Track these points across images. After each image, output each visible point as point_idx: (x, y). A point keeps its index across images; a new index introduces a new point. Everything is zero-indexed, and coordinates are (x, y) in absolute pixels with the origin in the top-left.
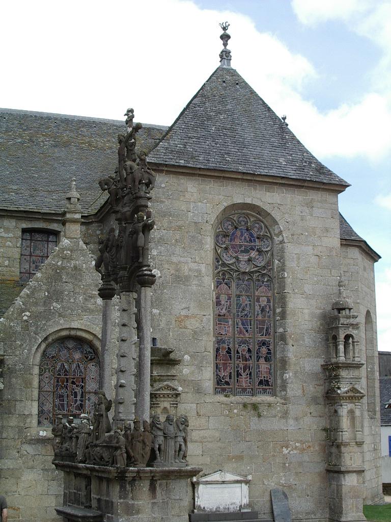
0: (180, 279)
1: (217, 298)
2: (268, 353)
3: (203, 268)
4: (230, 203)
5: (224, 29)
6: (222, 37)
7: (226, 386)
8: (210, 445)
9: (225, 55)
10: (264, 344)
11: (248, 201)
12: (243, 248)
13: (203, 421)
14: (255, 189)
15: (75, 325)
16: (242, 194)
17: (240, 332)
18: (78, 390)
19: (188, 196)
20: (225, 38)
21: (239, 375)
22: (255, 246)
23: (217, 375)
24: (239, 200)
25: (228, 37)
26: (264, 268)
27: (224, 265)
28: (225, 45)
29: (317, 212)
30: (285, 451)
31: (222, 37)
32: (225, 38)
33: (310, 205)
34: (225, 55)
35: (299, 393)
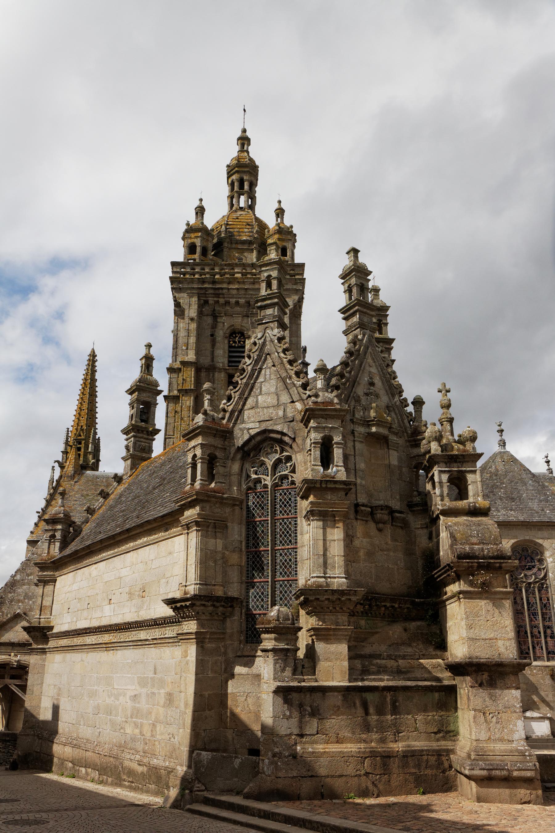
2: (552, 633)
7: (527, 655)
10: (548, 628)
11: (527, 538)
12: (527, 567)
14: (531, 530)
22: (535, 565)
23: (520, 648)
25: (502, 431)
26: (542, 579)
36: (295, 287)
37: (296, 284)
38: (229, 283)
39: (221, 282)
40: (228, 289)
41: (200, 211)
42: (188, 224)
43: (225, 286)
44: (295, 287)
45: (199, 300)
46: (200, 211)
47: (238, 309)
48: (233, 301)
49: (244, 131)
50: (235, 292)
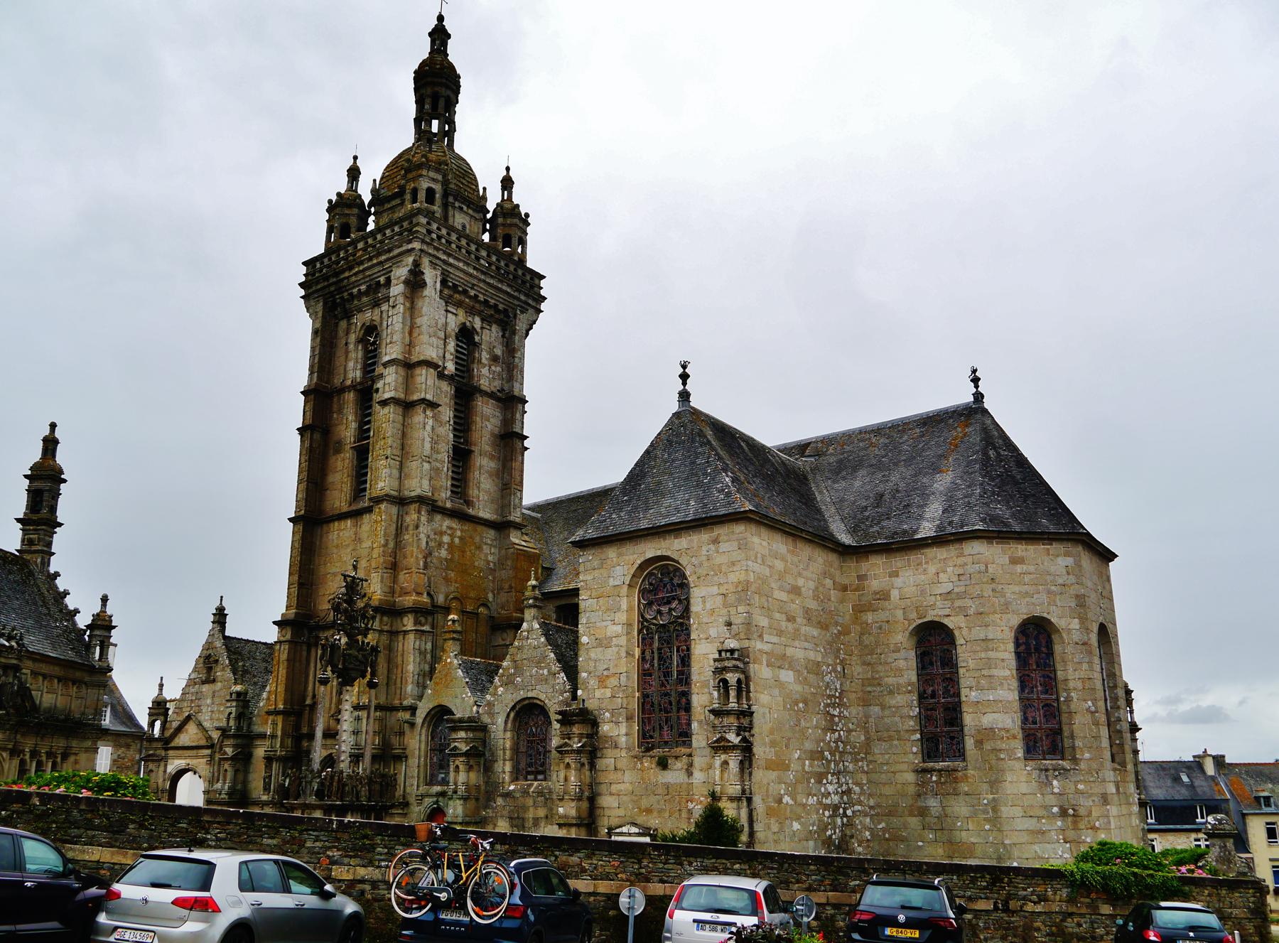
0: (603, 643)
1: (643, 652)
3: (618, 629)
4: (642, 559)
5: (684, 367)
6: (680, 376)
8: (625, 798)
9: (684, 396)
11: (659, 553)
13: (620, 773)
15: (530, 695)
16: (651, 549)
17: (663, 685)
18: (541, 749)
19: (609, 562)
20: (684, 377)
21: (661, 728)
24: (649, 555)
25: (688, 376)
26: (682, 617)
27: (646, 620)
28: (684, 384)
29: (724, 547)
30: (690, 806)
31: (680, 376)
32: (684, 377)
33: (716, 541)
34: (684, 396)
35: (704, 744)
36: (410, 246)
37: (410, 242)
38: (351, 268)
39: (343, 271)
40: (348, 278)
41: (354, 173)
42: (330, 201)
43: (347, 274)
44: (410, 246)
45: (325, 304)
46: (354, 173)
47: (365, 299)
48: (355, 290)
49: (441, 18)
50: (353, 279)
